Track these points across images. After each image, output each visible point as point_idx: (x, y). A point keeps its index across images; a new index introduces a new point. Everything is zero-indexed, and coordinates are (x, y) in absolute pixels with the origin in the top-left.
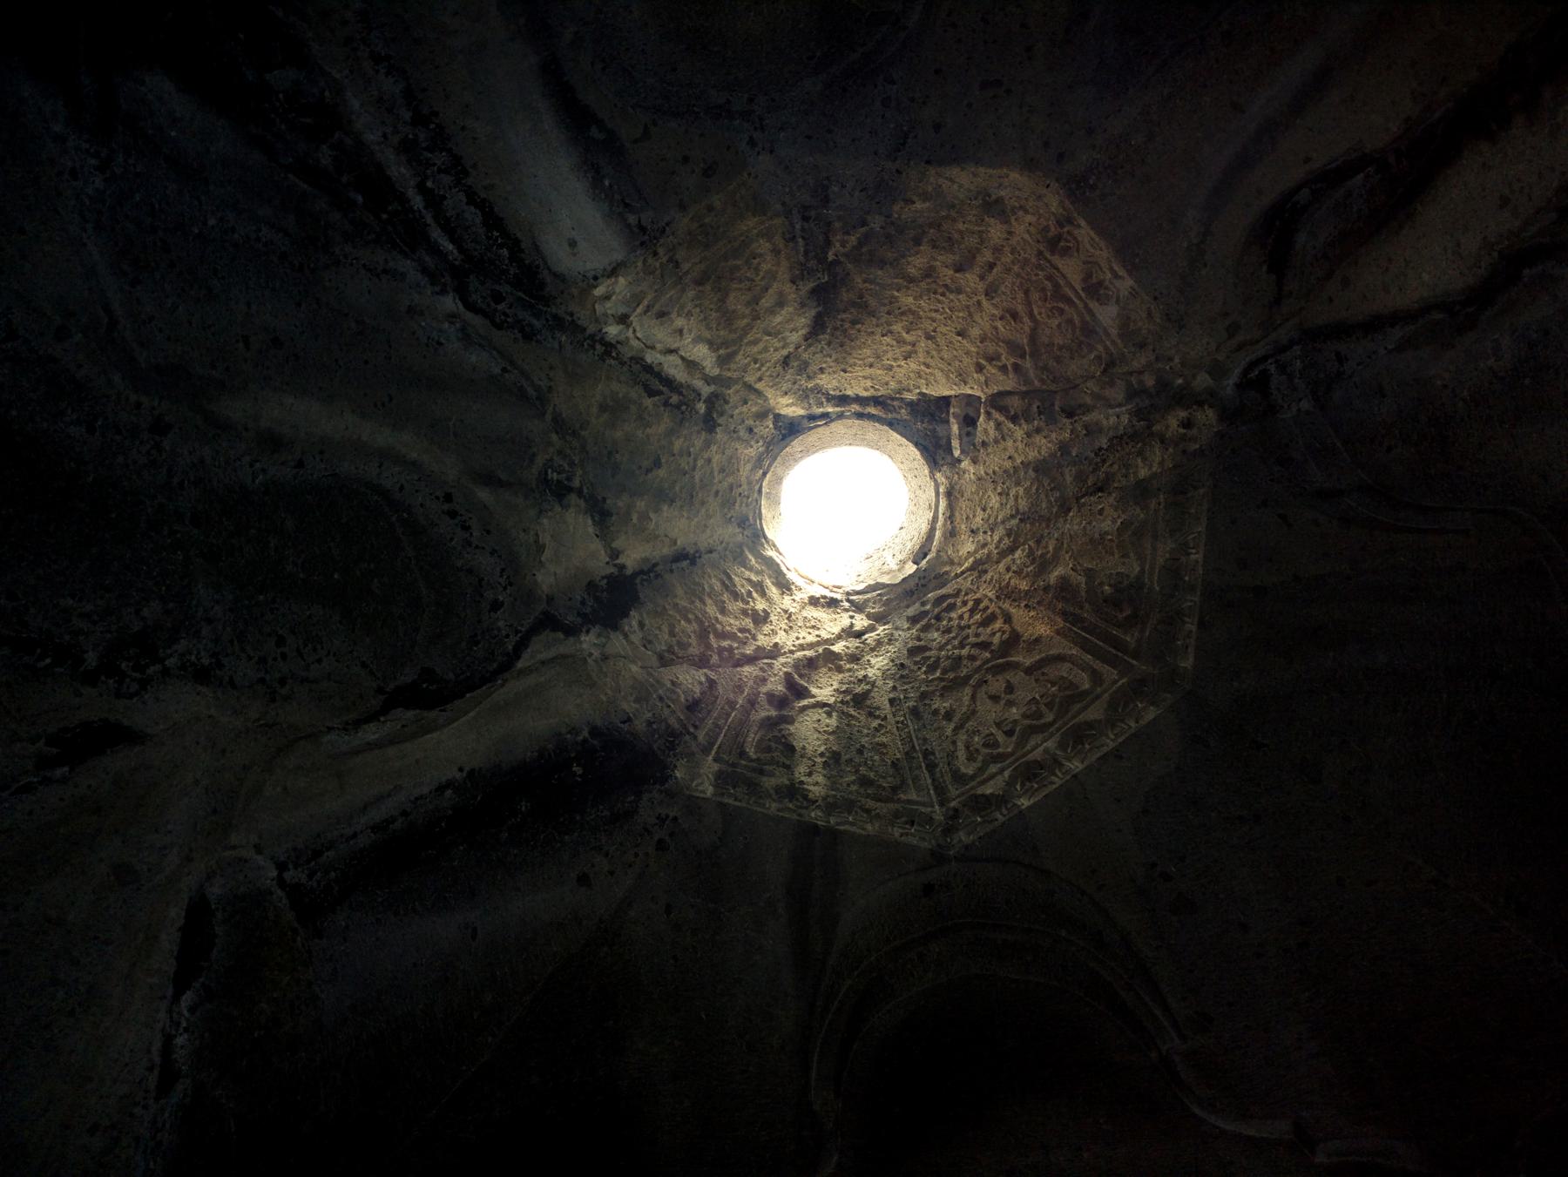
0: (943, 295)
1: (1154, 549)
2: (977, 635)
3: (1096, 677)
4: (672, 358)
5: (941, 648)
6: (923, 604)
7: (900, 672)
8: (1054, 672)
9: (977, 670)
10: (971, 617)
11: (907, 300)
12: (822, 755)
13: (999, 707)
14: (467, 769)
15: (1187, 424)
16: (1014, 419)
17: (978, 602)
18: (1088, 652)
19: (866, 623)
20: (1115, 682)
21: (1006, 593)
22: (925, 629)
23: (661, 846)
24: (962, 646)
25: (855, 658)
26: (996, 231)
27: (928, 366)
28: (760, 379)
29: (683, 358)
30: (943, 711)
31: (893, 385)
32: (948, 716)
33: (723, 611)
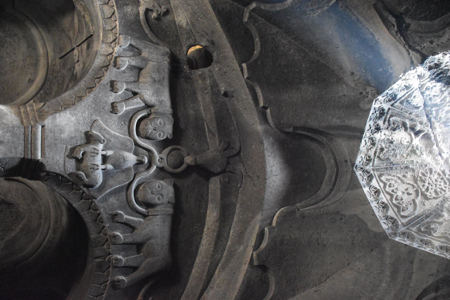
2: (432, 189)
5: (430, 178)
9: (419, 187)
10: (439, 188)
12: (392, 139)
14: (379, 40)
20: (400, 221)
22: (439, 174)
23: (361, 93)
24: (429, 184)
25: (431, 152)
30: (406, 175)
32: (404, 176)
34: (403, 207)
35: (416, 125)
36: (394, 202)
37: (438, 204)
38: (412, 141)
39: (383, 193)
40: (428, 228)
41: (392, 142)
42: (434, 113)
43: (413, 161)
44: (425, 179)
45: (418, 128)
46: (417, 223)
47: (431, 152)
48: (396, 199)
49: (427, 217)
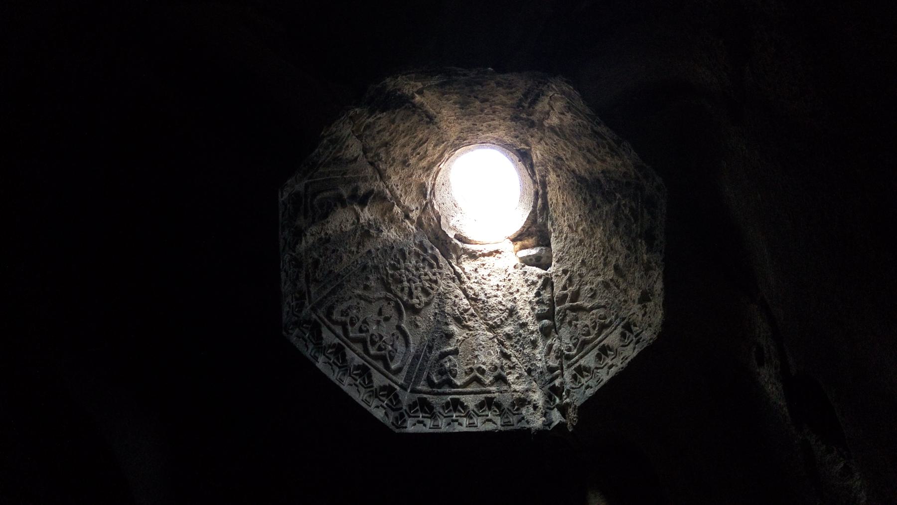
0: (603, 254)
2: (416, 288)
3: (398, 371)
4: (547, 108)
5: (407, 269)
6: (432, 249)
7: (389, 249)
9: (396, 296)
11: (599, 233)
12: (326, 234)
13: (376, 317)
16: (538, 294)
17: (436, 282)
19: (415, 218)
20: (396, 383)
21: (443, 297)
22: (417, 255)
24: (409, 281)
25: (392, 220)
26: (635, 293)
27: (566, 238)
31: (554, 216)
32: (366, 288)
33: (404, 146)
34: (390, 351)
35: (356, 189)
36: (373, 351)
37: (436, 314)
38: (358, 219)
39: (349, 346)
40: (442, 372)
41: (328, 240)
42: (383, 155)
43: (370, 252)
44: (401, 275)
45: (362, 192)
47: (392, 220)
48: (373, 343)
49: (430, 348)
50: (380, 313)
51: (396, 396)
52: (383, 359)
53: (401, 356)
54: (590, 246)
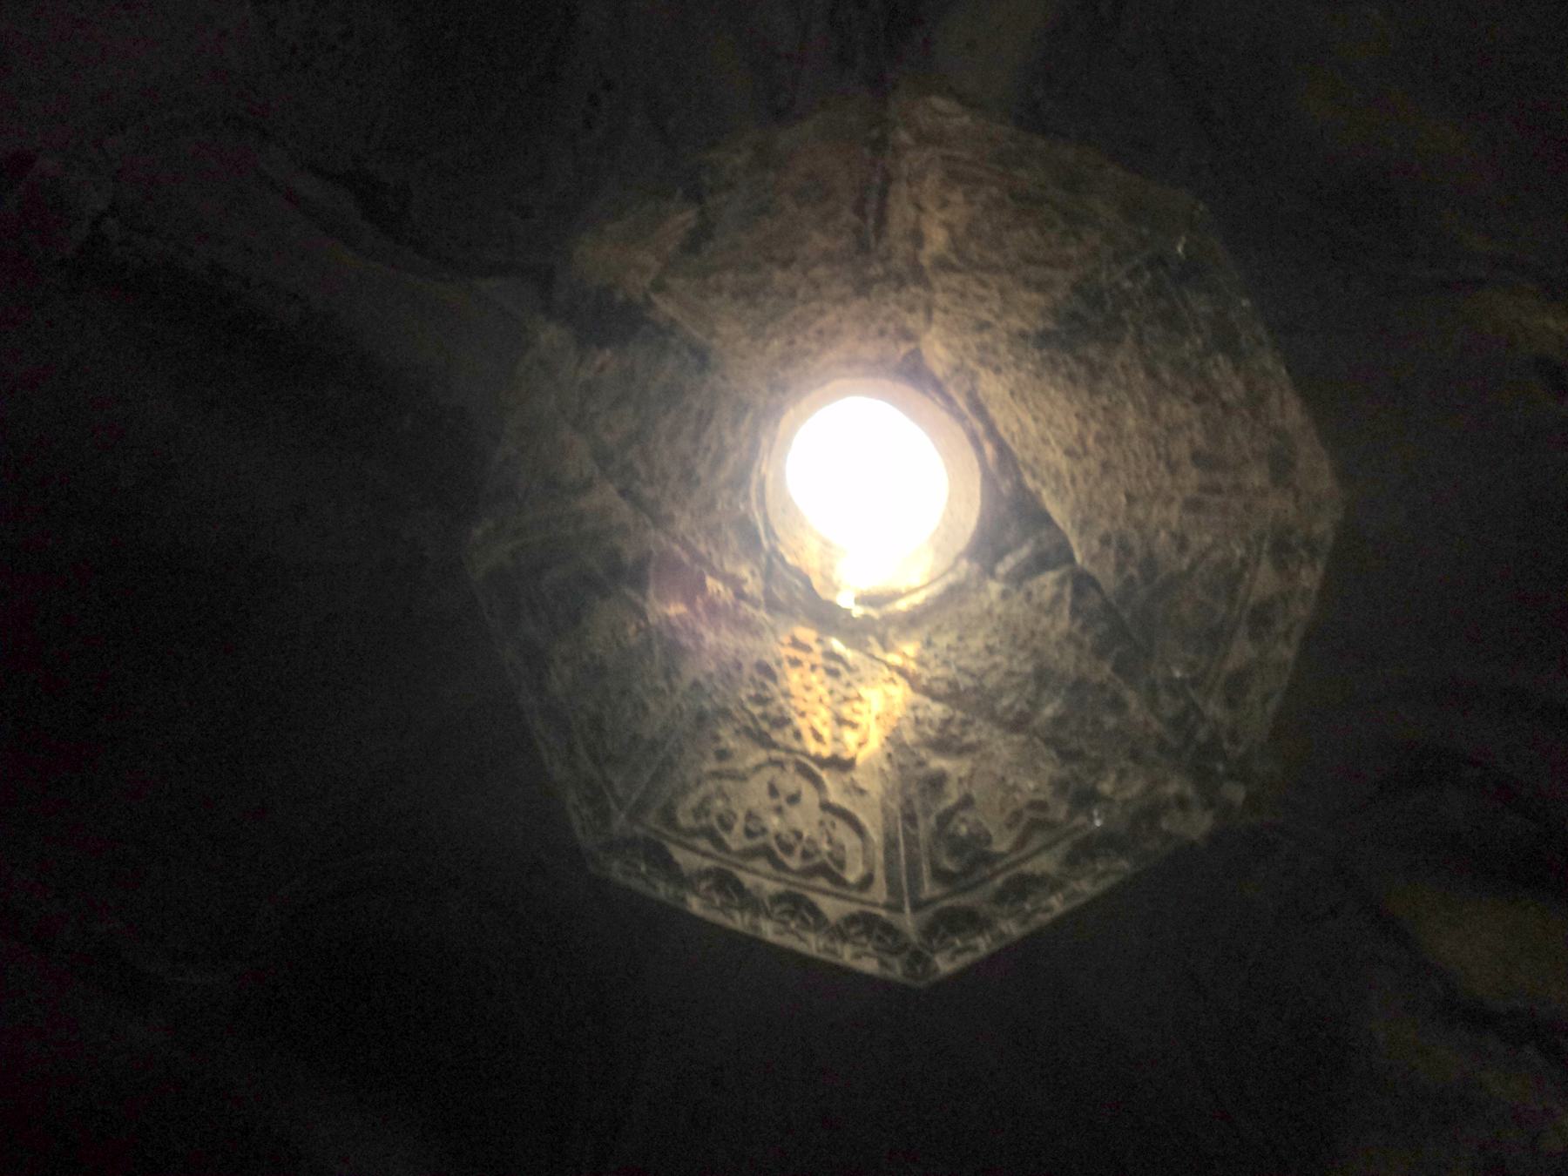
0: (1159, 456)
1: (1037, 852)
3: (867, 882)
4: (911, 212)
8: (843, 833)
9: (789, 750)
12: (592, 656)
13: (768, 802)
15: (1182, 802)
16: (1075, 611)
18: (886, 852)
26: (1257, 477)
27: (1073, 480)
28: (946, 311)
29: (918, 218)
32: (723, 755)
40: (958, 847)
46: (913, 865)
48: (788, 849)
50: (773, 791)
51: (888, 928)
52: (823, 870)
53: (859, 857)
54: (1126, 460)
